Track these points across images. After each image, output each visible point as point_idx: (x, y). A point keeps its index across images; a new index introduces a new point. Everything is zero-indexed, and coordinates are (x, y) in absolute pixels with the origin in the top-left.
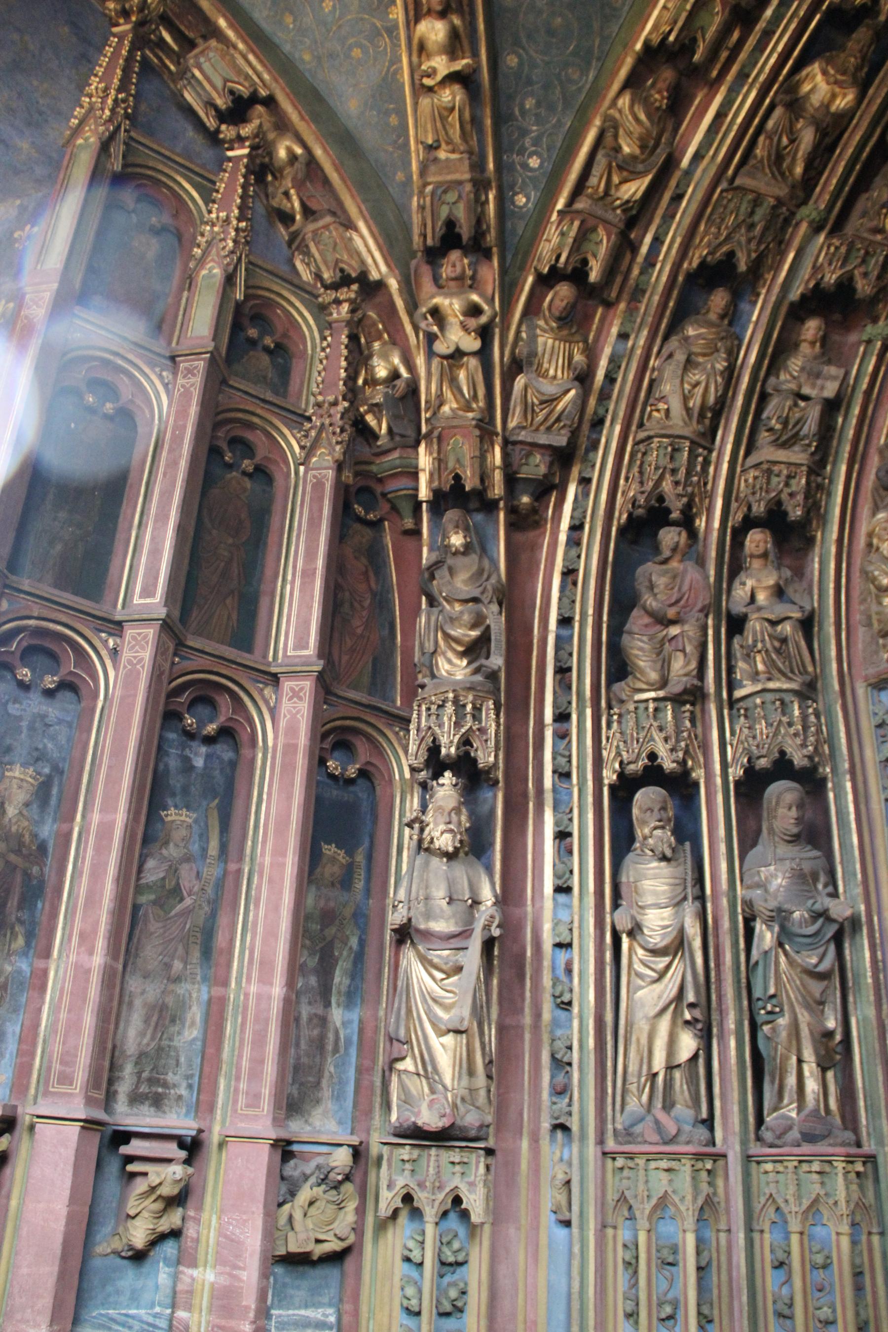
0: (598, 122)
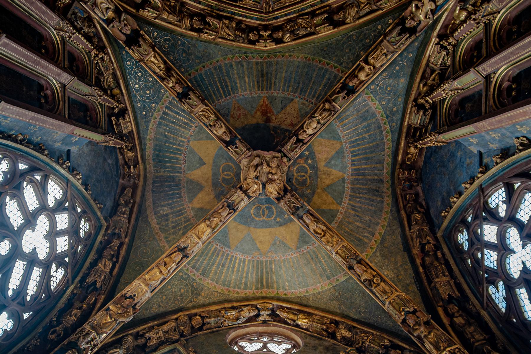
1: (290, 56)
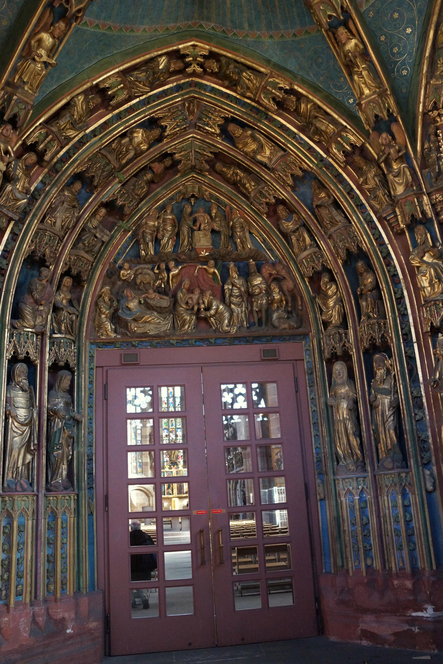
0: (69, 98)
1: (156, 30)
